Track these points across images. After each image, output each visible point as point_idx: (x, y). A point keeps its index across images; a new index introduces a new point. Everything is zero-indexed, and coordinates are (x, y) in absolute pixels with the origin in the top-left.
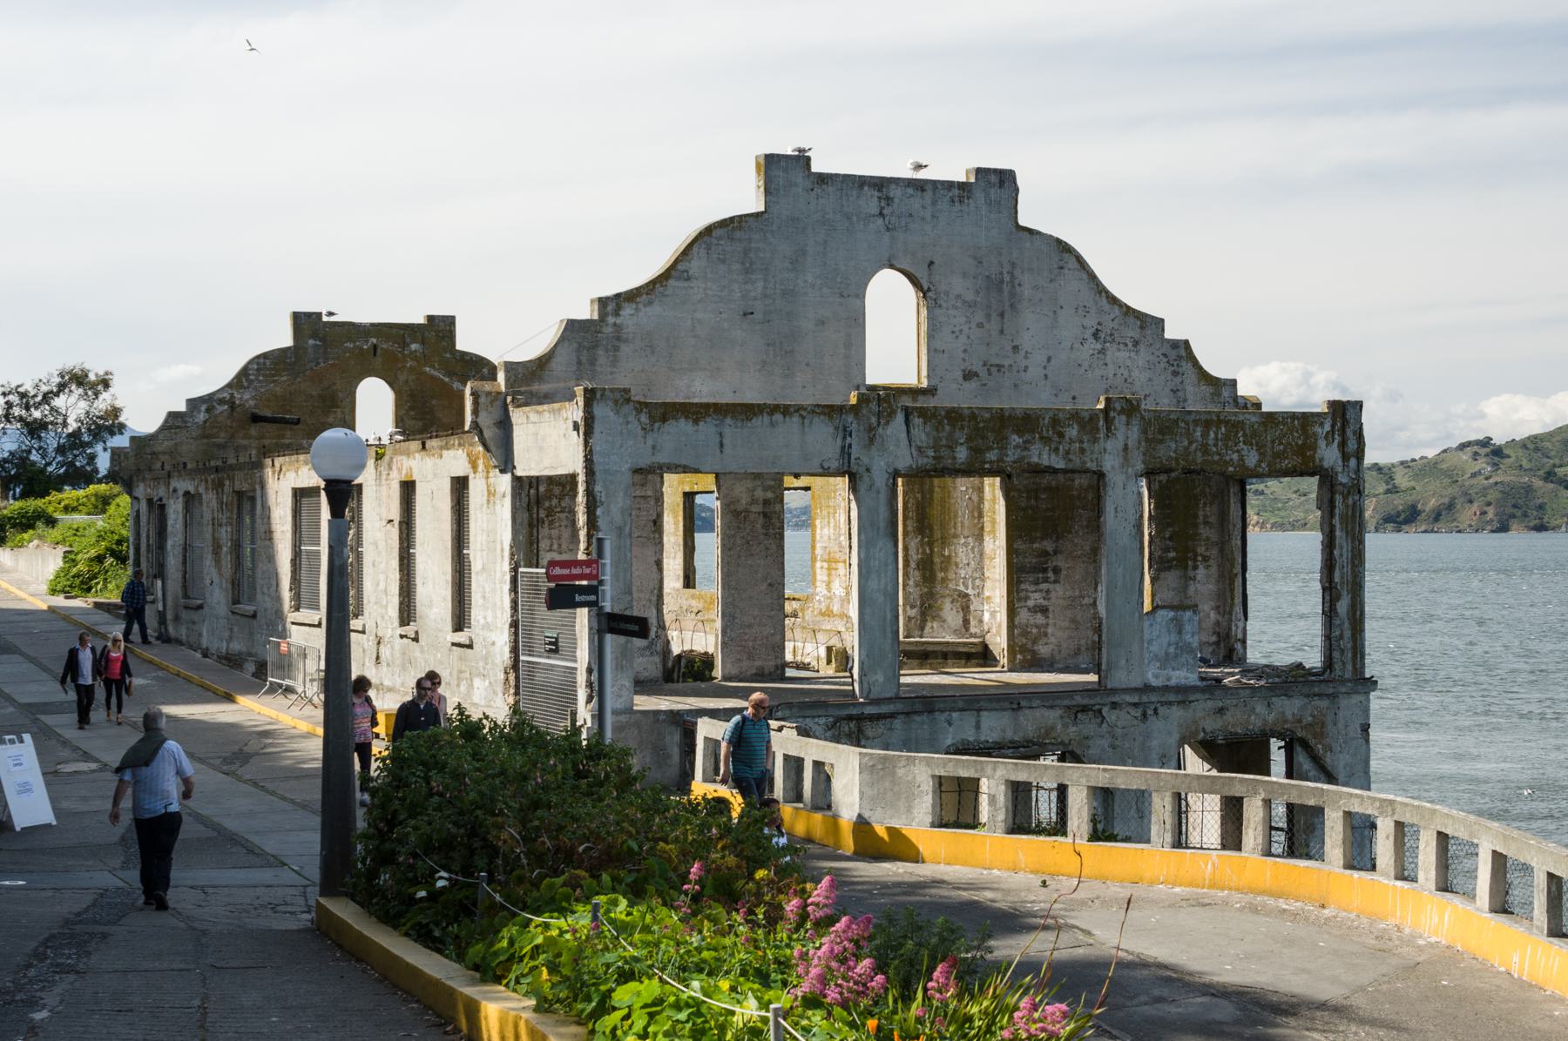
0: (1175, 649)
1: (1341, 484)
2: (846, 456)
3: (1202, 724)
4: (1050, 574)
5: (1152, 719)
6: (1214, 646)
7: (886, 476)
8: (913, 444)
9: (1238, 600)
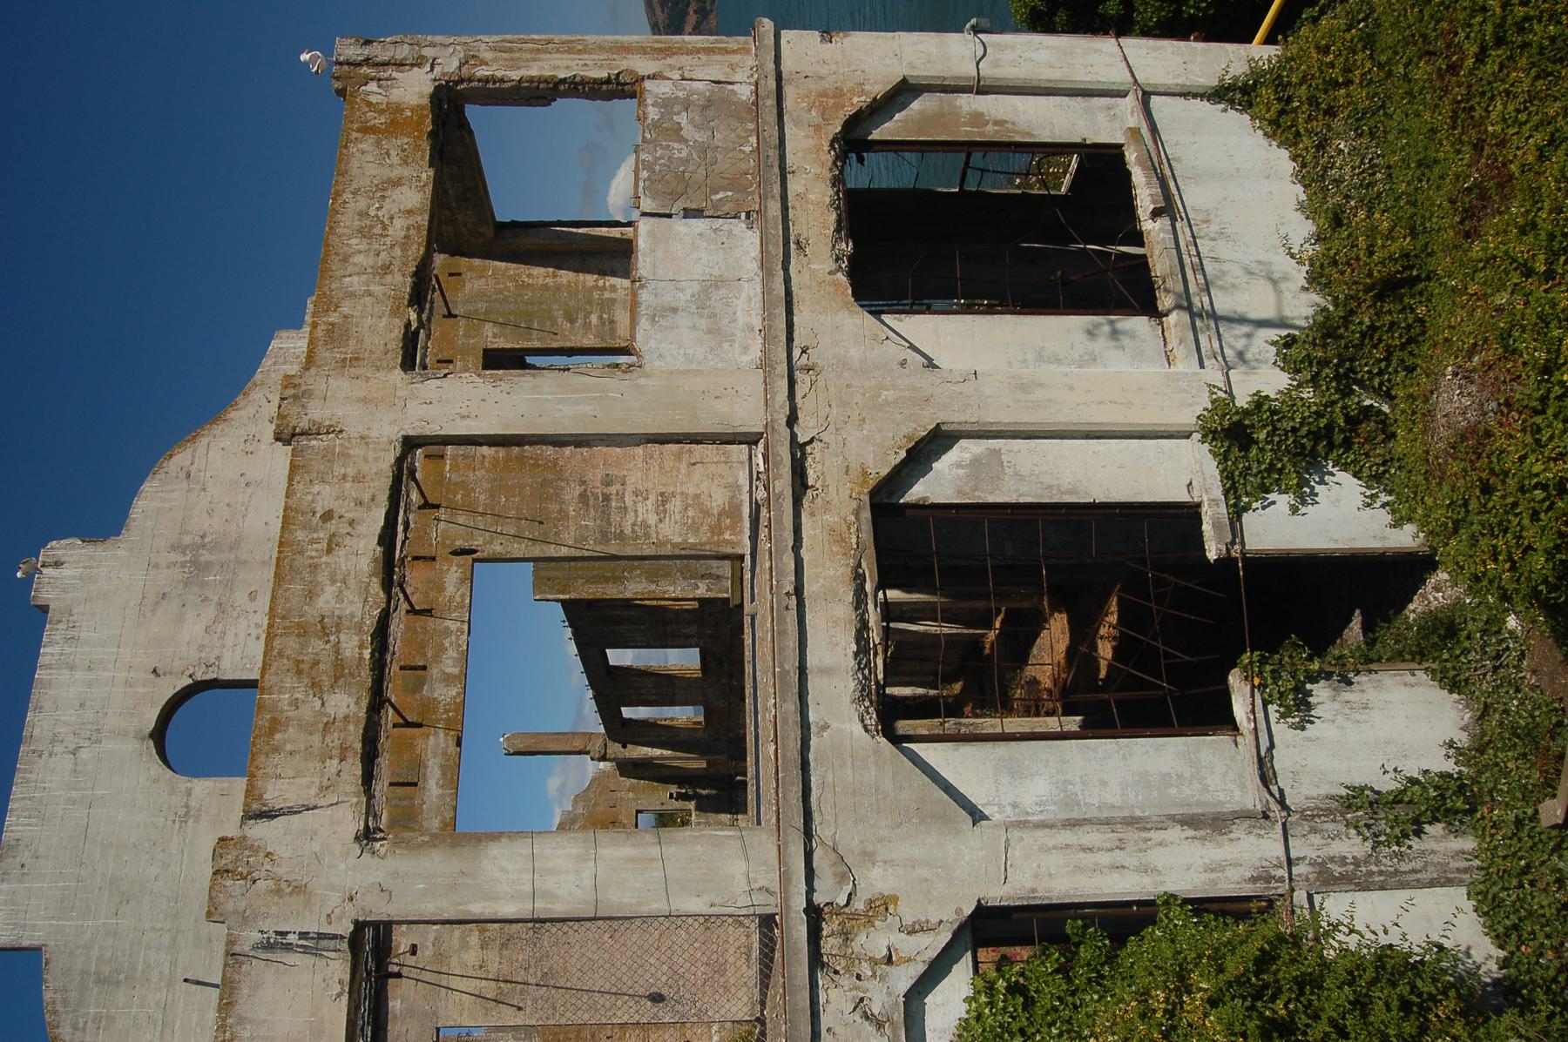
1: (460, 68)
4: (613, 490)
8: (312, 803)
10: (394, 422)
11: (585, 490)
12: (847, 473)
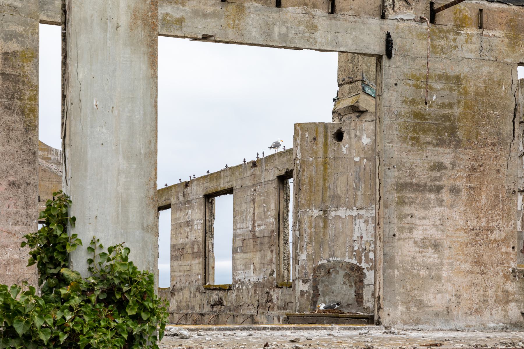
11: (446, 168)
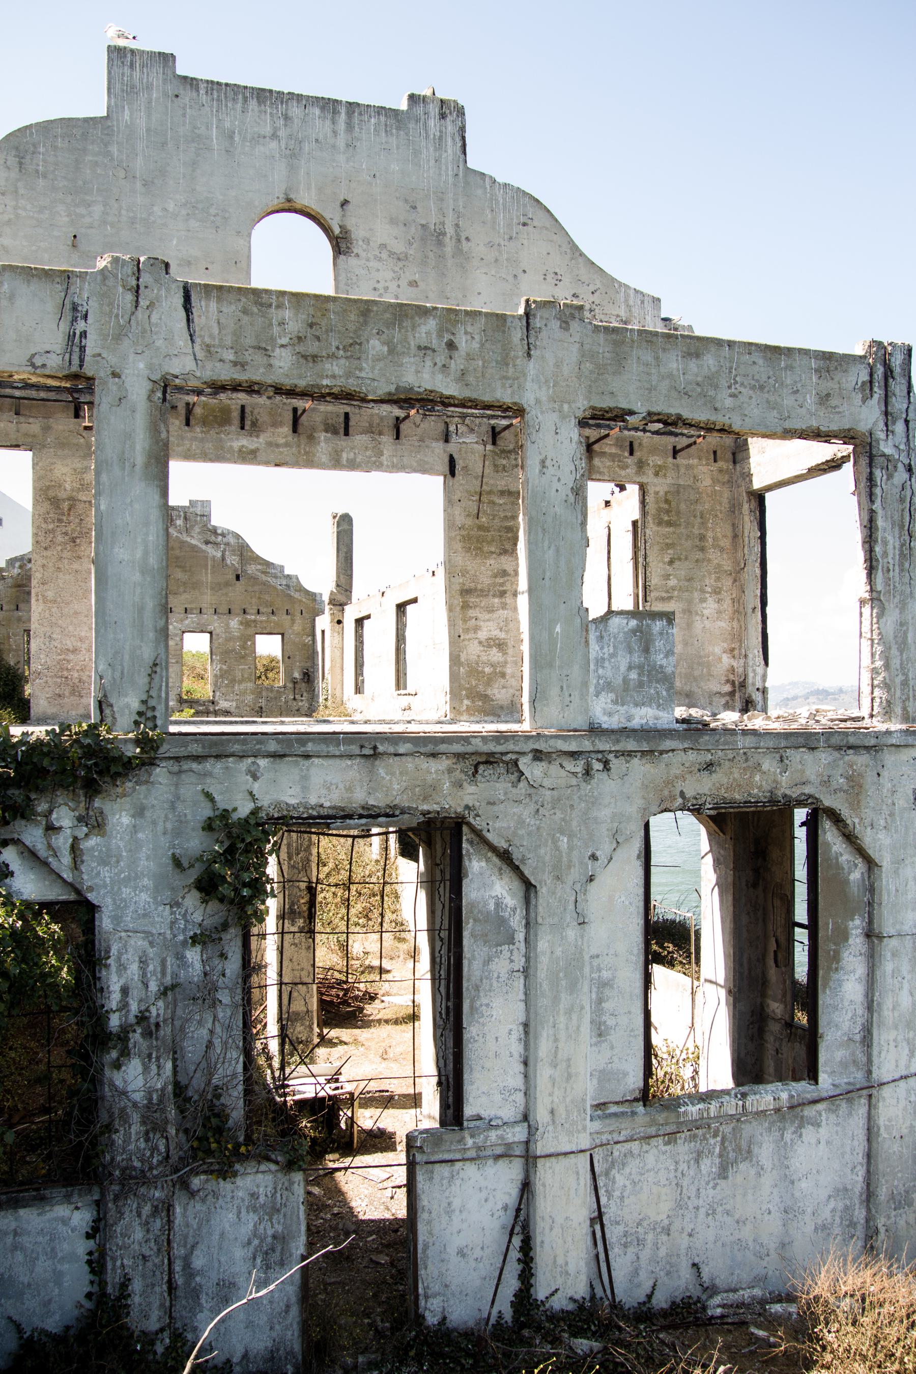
0: (639, 675)
2: (77, 349)
3: (679, 786)
5: (599, 776)
6: (728, 698)
7: (149, 386)
8: (198, 340)
9: (757, 640)
10: (538, 401)
11: (509, 575)
12: (489, 803)
